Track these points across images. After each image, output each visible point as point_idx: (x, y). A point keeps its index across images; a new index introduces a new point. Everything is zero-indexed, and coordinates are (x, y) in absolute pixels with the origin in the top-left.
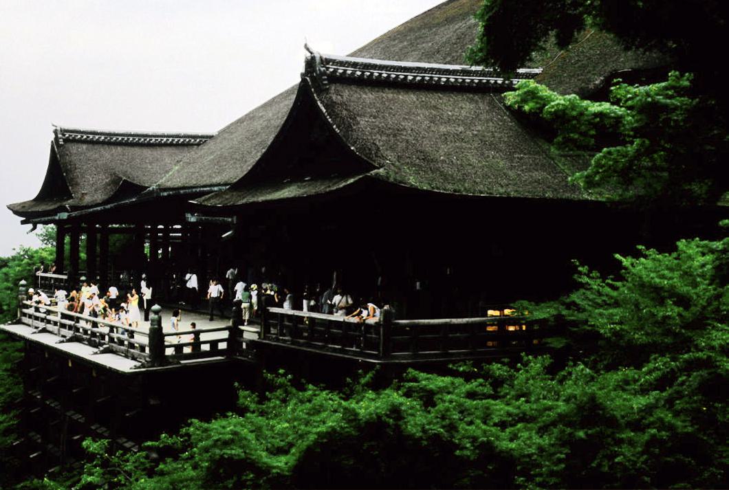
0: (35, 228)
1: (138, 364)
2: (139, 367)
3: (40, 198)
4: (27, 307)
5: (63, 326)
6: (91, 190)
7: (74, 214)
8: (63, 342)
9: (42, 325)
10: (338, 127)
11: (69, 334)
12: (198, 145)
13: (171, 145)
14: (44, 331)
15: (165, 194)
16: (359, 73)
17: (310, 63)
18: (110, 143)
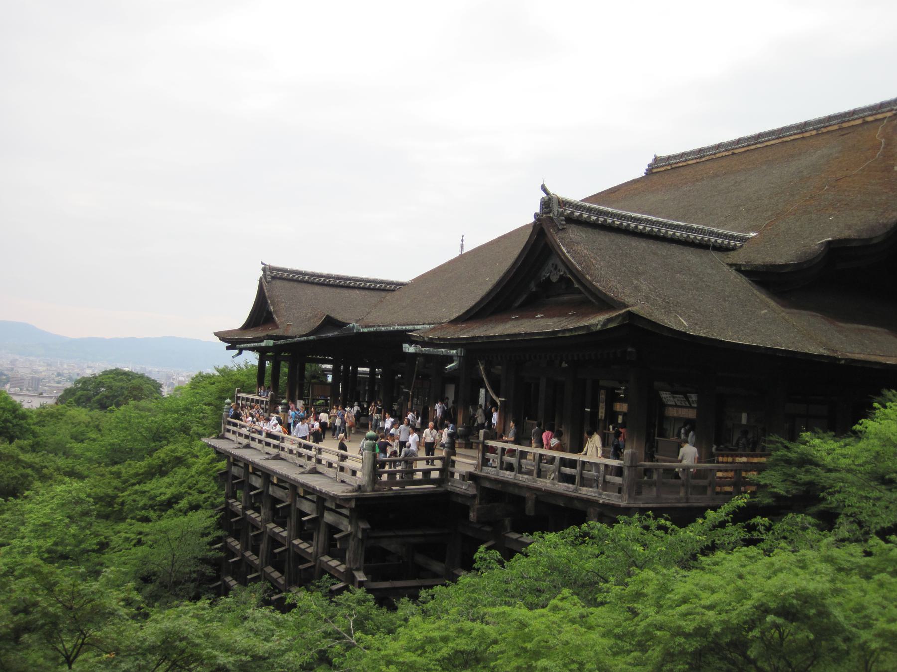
0: (240, 353)
1: (350, 488)
2: (351, 492)
4: (229, 423)
5: (268, 444)
6: (296, 322)
7: (279, 342)
8: (267, 459)
9: (245, 441)
10: (580, 264)
12: (393, 290)
13: (369, 289)
14: (247, 446)
15: (366, 330)
16: (594, 218)
17: (547, 203)
18: (313, 283)
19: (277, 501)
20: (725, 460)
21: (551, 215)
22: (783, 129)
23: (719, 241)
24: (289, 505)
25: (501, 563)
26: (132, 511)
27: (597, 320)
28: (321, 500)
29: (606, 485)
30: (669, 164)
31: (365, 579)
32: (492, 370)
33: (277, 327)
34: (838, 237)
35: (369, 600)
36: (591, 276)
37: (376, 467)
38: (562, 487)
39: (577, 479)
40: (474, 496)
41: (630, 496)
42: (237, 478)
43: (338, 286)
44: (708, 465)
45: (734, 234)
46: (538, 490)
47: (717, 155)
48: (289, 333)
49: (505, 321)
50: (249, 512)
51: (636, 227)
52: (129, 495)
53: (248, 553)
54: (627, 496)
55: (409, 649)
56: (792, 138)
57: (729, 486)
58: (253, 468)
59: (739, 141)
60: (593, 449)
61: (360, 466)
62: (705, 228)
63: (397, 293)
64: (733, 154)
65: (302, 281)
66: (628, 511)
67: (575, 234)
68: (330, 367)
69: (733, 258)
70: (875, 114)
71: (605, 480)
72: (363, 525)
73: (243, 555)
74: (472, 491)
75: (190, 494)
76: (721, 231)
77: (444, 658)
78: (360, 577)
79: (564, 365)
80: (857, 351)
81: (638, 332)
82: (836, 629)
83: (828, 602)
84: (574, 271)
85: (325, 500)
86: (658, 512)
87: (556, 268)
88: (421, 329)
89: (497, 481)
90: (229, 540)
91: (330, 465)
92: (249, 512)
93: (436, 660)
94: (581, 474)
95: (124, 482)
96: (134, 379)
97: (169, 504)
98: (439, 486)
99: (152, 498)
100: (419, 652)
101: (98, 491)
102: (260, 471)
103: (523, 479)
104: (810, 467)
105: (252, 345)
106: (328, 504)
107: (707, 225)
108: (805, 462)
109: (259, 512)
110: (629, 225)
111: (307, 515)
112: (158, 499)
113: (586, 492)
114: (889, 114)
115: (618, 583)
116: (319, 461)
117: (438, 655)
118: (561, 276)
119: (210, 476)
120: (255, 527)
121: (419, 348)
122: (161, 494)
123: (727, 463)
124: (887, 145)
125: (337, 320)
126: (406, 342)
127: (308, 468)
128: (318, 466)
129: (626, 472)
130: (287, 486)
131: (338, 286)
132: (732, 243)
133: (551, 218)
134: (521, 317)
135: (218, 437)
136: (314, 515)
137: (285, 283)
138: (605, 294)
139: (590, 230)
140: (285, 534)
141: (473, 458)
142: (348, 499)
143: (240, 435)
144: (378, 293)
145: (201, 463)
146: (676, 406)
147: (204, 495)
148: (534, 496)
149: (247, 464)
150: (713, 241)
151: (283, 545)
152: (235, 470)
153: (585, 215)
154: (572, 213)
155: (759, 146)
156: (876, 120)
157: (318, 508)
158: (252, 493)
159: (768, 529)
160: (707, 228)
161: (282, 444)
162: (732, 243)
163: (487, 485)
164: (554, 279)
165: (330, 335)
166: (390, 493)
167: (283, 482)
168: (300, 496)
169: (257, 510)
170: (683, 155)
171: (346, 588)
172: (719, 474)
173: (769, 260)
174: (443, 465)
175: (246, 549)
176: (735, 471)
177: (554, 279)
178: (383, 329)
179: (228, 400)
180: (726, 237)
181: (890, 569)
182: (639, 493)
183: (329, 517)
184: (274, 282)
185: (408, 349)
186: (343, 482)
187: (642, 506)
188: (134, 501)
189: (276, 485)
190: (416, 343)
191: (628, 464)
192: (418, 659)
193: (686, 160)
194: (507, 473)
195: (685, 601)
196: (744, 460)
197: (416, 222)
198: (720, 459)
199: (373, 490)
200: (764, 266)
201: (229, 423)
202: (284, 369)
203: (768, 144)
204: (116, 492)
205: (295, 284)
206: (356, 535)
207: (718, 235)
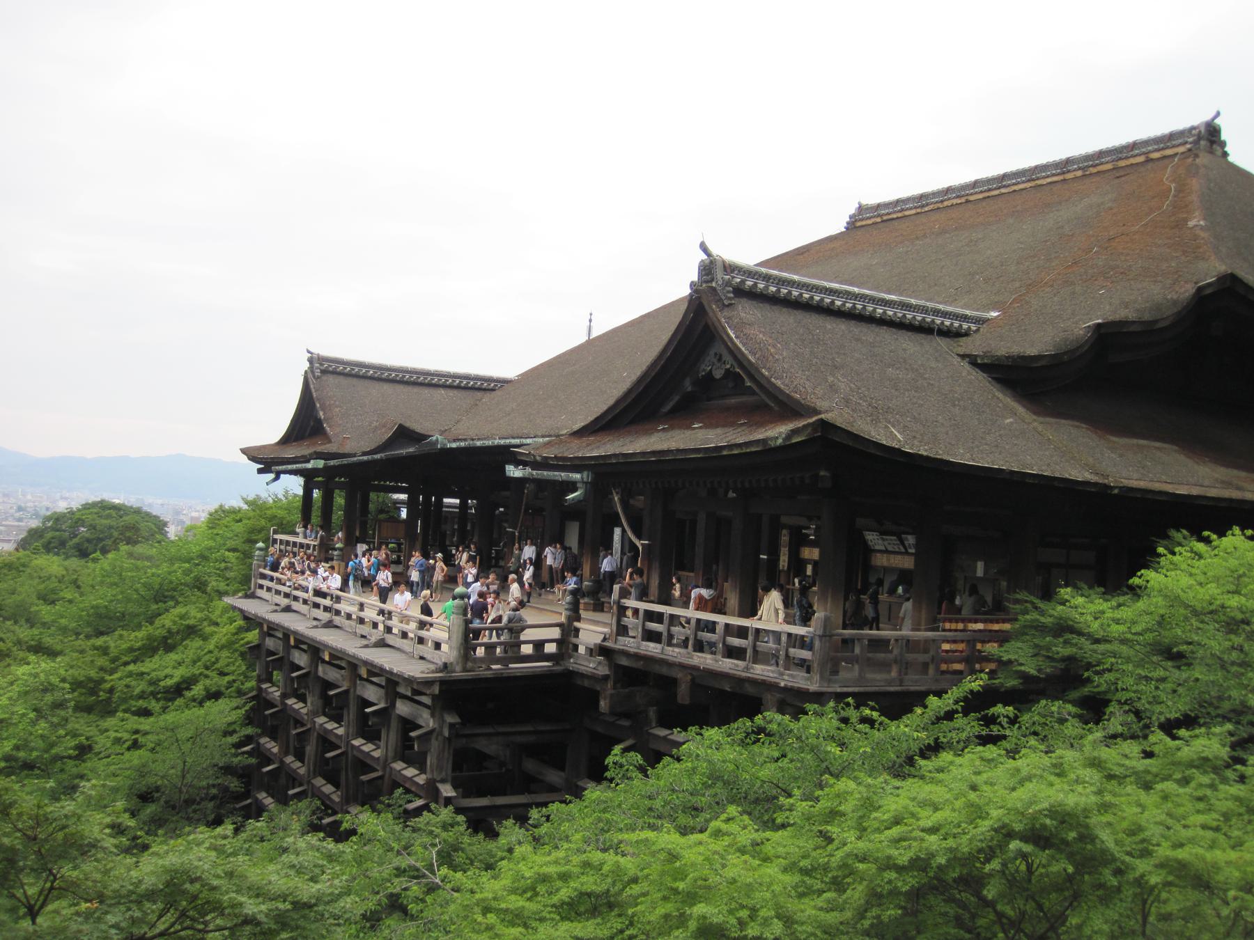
0: (277, 478)
1: (432, 667)
3: (286, 440)
4: (263, 576)
5: (317, 606)
6: (356, 433)
7: (332, 463)
8: (316, 627)
9: (285, 602)
11: (325, 616)
12: (493, 390)
13: (458, 387)
14: (288, 609)
15: (454, 445)
16: (774, 289)
17: (709, 268)
18: (380, 379)
19: (329, 685)
20: (953, 626)
21: (714, 284)
22: (1036, 167)
23: (947, 323)
24: (347, 692)
25: (642, 770)
26: (124, 700)
27: (777, 432)
28: (392, 684)
29: (791, 663)
30: (879, 216)
31: (454, 794)
32: (632, 502)
33: (330, 442)
34: (1111, 318)
35: (458, 824)
36: (769, 370)
37: (469, 636)
38: (727, 665)
39: (749, 653)
40: (606, 678)
41: (822, 677)
42: (273, 654)
43: (415, 384)
44: (930, 634)
45: (968, 312)
46: (695, 668)
47: (946, 204)
48: (347, 449)
49: (648, 432)
50: (290, 702)
51: (833, 302)
52: (120, 679)
53: (289, 759)
54: (817, 677)
55: (514, 891)
56: (1049, 180)
57: (959, 662)
58: (296, 640)
59: (976, 184)
60: (772, 612)
61: (446, 635)
62: (928, 304)
63: (498, 393)
64: (967, 201)
65: (365, 377)
66: (819, 698)
67: (747, 311)
68: (403, 497)
69: (966, 345)
70: (1163, 149)
71: (787, 655)
72: (451, 719)
73: (282, 762)
74: (604, 670)
75: (207, 677)
76: (950, 309)
77: (563, 903)
78: (447, 791)
79: (731, 495)
80: (1135, 476)
81: (833, 449)
82: (1105, 858)
83: (1093, 821)
84: (745, 363)
85: (396, 683)
86: (861, 699)
87: (720, 360)
88: (532, 444)
89: (637, 657)
90: (263, 740)
91: (404, 635)
92: (290, 702)
93: (552, 906)
94: (754, 647)
95: (113, 660)
96: (127, 514)
97: (178, 690)
98: (557, 664)
99: (153, 683)
100: (529, 895)
101: (76, 673)
102: (305, 643)
103: (675, 653)
104: (1070, 636)
105: (294, 467)
106: (401, 690)
107: (930, 300)
108: (1064, 629)
109: (305, 701)
110: (822, 300)
111: (373, 704)
112: (162, 684)
113: (761, 671)
114: (1181, 149)
115: (806, 798)
116: (389, 630)
117: (555, 899)
118: (727, 370)
119: (236, 650)
120: (299, 722)
121: (528, 470)
122: (166, 677)
123: (956, 630)
124: (1179, 190)
125: (413, 432)
126: (510, 463)
127: (373, 639)
128: (387, 636)
129: (817, 644)
130: (343, 664)
131: (415, 384)
132: (965, 326)
133: (714, 289)
134: (672, 428)
135: (246, 596)
136: (382, 705)
137: (341, 379)
138: (788, 396)
139: (767, 306)
140: (341, 731)
141: (605, 624)
142: (429, 683)
143: (278, 592)
144: (470, 393)
145: (223, 632)
146: (886, 551)
147: (227, 678)
148: (689, 677)
149: (287, 634)
150: (938, 322)
151: (338, 747)
152: (270, 643)
153: (761, 286)
154: (743, 282)
155: (1003, 190)
156: (1165, 157)
157: (387, 694)
158: (294, 675)
159: (1013, 721)
160: (930, 305)
161: (337, 606)
162: (965, 326)
163: (624, 662)
164: (718, 374)
165: (403, 452)
166: (488, 674)
167: (338, 660)
168: (361, 679)
169: (302, 698)
170: (898, 202)
171: (426, 807)
172: (946, 647)
173: (1016, 350)
174: (563, 635)
175: (287, 753)
176: (968, 642)
177: (718, 374)
178: (479, 443)
179: (260, 545)
180: (956, 316)
181: (1178, 776)
182: (835, 672)
183: (402, 708)
184: (324, 378)
185: (514, 472)
186: (422, 658)
187: (839, 690)
188: (127, 686)
189: (329, 663)
190: (525, 464)
191: (820, 632)
192: (527, 904)
193: (902, 210)
194: (652, 645)
195: (897, 821)
196: (980, 626)
197: (523, 293)
198: (947, 626)
199: (465, 670)
200: (1007, 358)
201: (263, 576)
202: (339, 500)
203: (1016, 188)
204: (102, 674)
205: (355, 381)
206: (441, 733)
207: (945, 314)
